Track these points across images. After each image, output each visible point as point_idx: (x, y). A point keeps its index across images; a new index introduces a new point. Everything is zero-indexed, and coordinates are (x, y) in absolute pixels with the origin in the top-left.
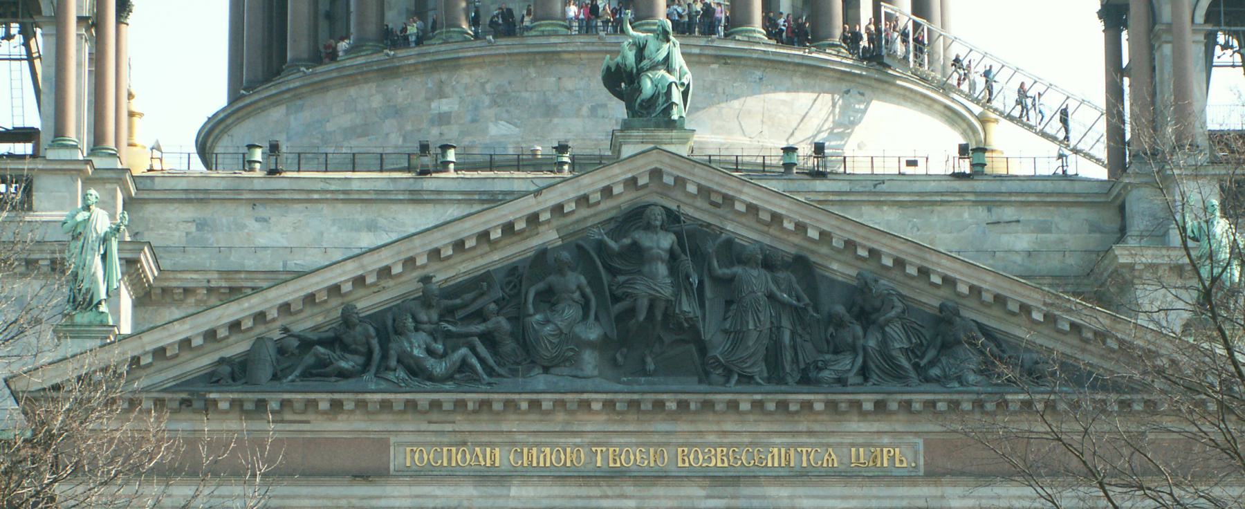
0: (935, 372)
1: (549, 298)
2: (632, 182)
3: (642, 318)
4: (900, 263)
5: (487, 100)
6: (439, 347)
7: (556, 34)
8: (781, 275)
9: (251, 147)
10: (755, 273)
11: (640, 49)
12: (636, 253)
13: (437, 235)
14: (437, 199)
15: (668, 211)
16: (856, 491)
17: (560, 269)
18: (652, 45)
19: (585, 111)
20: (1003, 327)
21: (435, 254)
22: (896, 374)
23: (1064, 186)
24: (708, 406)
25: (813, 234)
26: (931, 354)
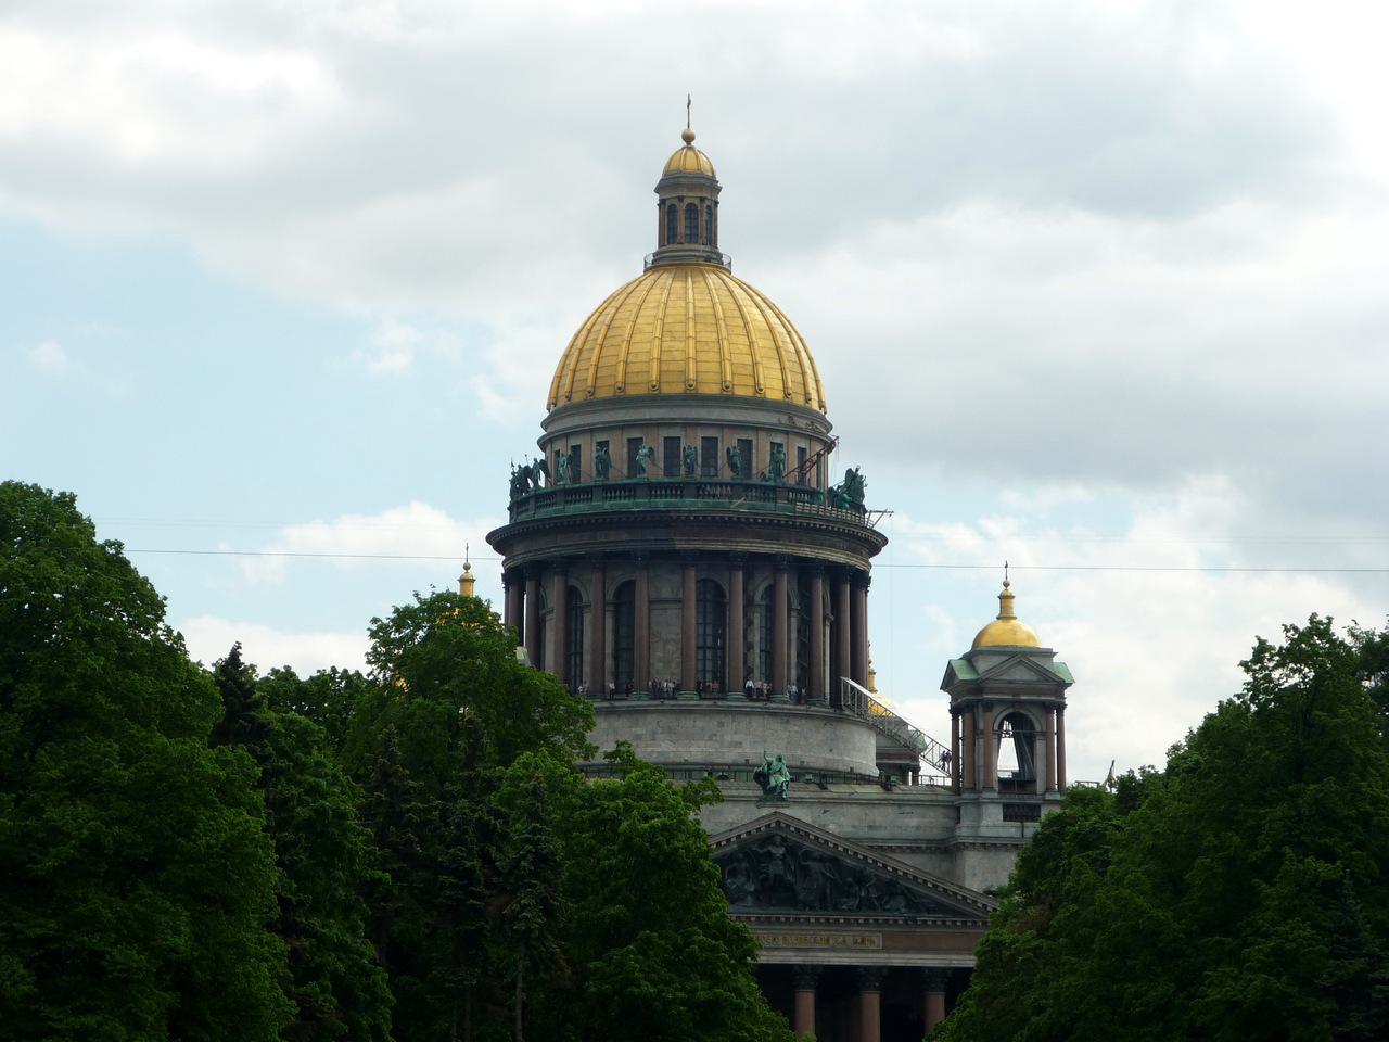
0: (887, 907)
4: (875, 862)
5: (660, 730)
8: (827, 864)
12: (770, 855)
17: (739, 861)
18: (775, 763)
20: (915, 888)
22: (872, 907)
26: (886, 899)
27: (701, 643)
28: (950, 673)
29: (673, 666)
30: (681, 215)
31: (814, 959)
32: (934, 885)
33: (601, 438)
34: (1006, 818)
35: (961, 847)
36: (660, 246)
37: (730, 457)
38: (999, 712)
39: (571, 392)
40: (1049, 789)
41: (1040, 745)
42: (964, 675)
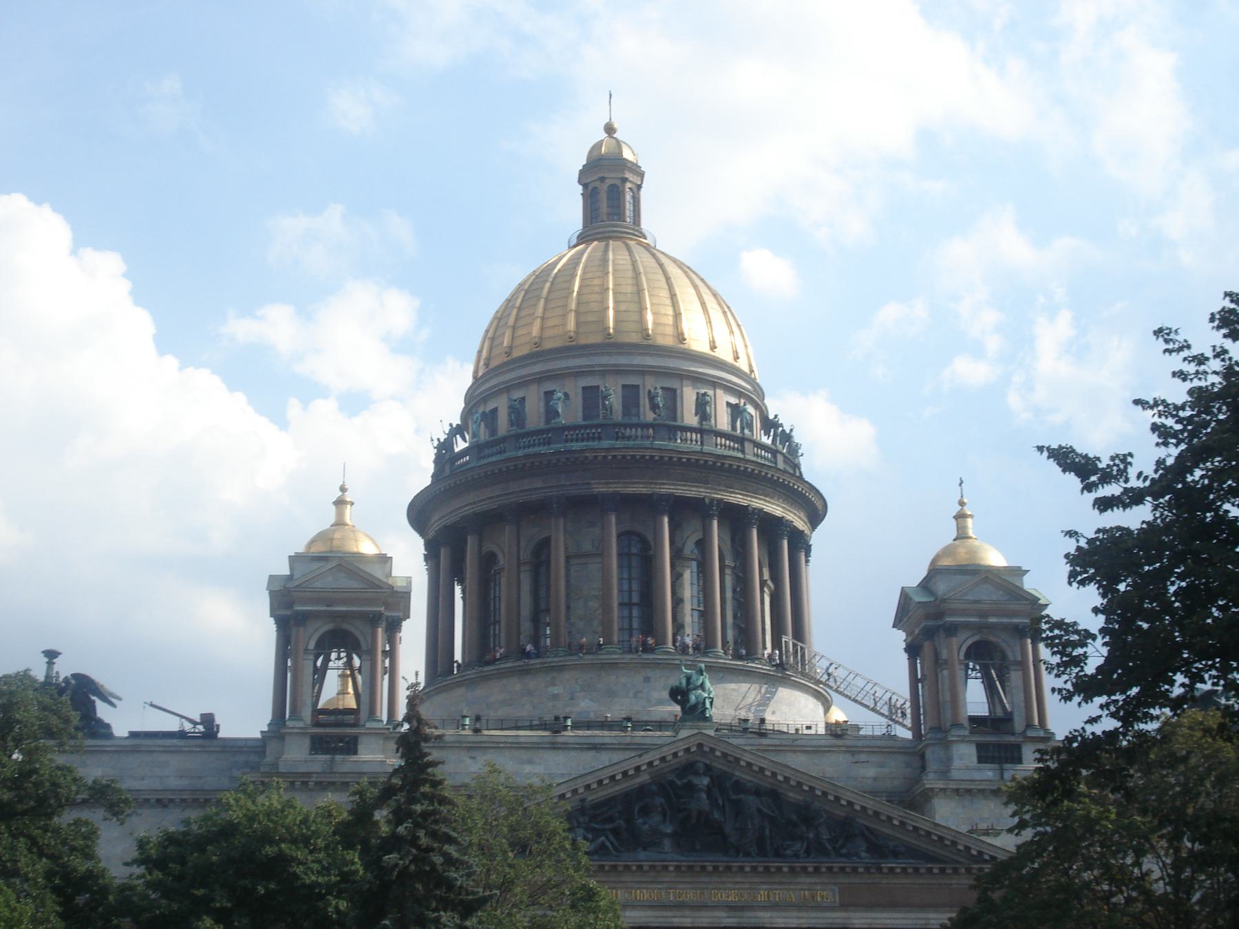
0: (844, 851)
1: (645, 811)
2: (687, 750)
3: (694, 821)
4: (825, 794)
5: (578, 688)
6: (590, 836)
7: (615, 653)
9: (464, 717)
10: (751, 798)
11: (689, 678)
12: (690, 787)
13: (589, 777)
14: (565, 747)
15: (706, 765)
16: (804, 914)
18: (694, 677)
19: (631, 695)
20: (878, 827)
21: (588, 787)
22: (822, 851)
23: (891, 743)
24: (729, 868)
25: (780, 778)
27: (626, 600)
28: (905, 596)
29: (596, 623)
30: (603, 196)
31: (753, 920)
32: (901, 822)
33: (517, 395)
34: (981, 760)
35: (928, 795)
36: (585, 226)
37: (652, 398)
38: (962, 636)
39: (488, 359)
40: (1029, 725)
41: (1015, 676)
42: (919, 598)
